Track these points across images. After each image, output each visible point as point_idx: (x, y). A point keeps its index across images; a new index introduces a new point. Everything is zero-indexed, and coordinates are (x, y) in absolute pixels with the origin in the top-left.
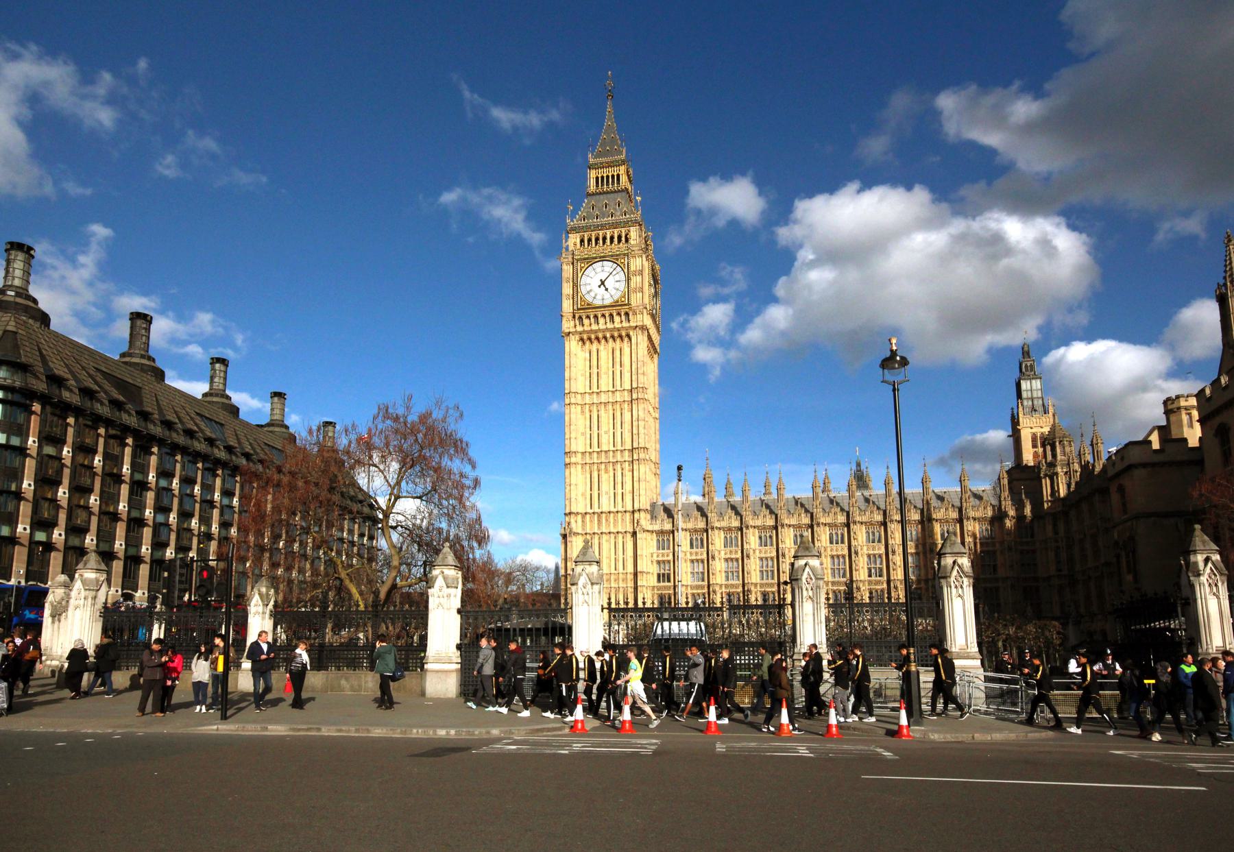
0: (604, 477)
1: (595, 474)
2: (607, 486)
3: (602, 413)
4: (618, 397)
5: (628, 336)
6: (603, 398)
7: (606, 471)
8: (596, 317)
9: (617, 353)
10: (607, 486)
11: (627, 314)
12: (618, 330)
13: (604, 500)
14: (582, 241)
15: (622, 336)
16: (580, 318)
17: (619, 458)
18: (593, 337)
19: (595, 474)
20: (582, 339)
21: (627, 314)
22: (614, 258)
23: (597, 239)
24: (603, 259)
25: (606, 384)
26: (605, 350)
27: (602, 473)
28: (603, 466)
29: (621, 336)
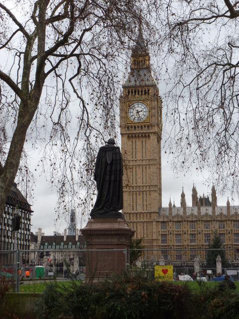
0: (138, 197)
1: (135, 196)
2: (140, 201)
3: (137, 169)
4: (144, 163)
5: (149, 136)
6: (138, 163)
7: (140, 195)
8: (135, 127)
9: (144, 143)
10: (140, 201)
11: (148, 127)
12: (145, 133)
13: (138, 207)
14: (129, 92)
15: (147, 136)
16: (128, 128)
17: (145, 189)
18: (134, 136)
19: (135, 196)
20: (128, 137)
21: (148, 127)
22: (143, 101)
23: (135, 92)
24: (138, 101)
25: (139, 157)
26: (139, 143)
27: (138, 195)
28: (138, 193)
29: (145, 136)
